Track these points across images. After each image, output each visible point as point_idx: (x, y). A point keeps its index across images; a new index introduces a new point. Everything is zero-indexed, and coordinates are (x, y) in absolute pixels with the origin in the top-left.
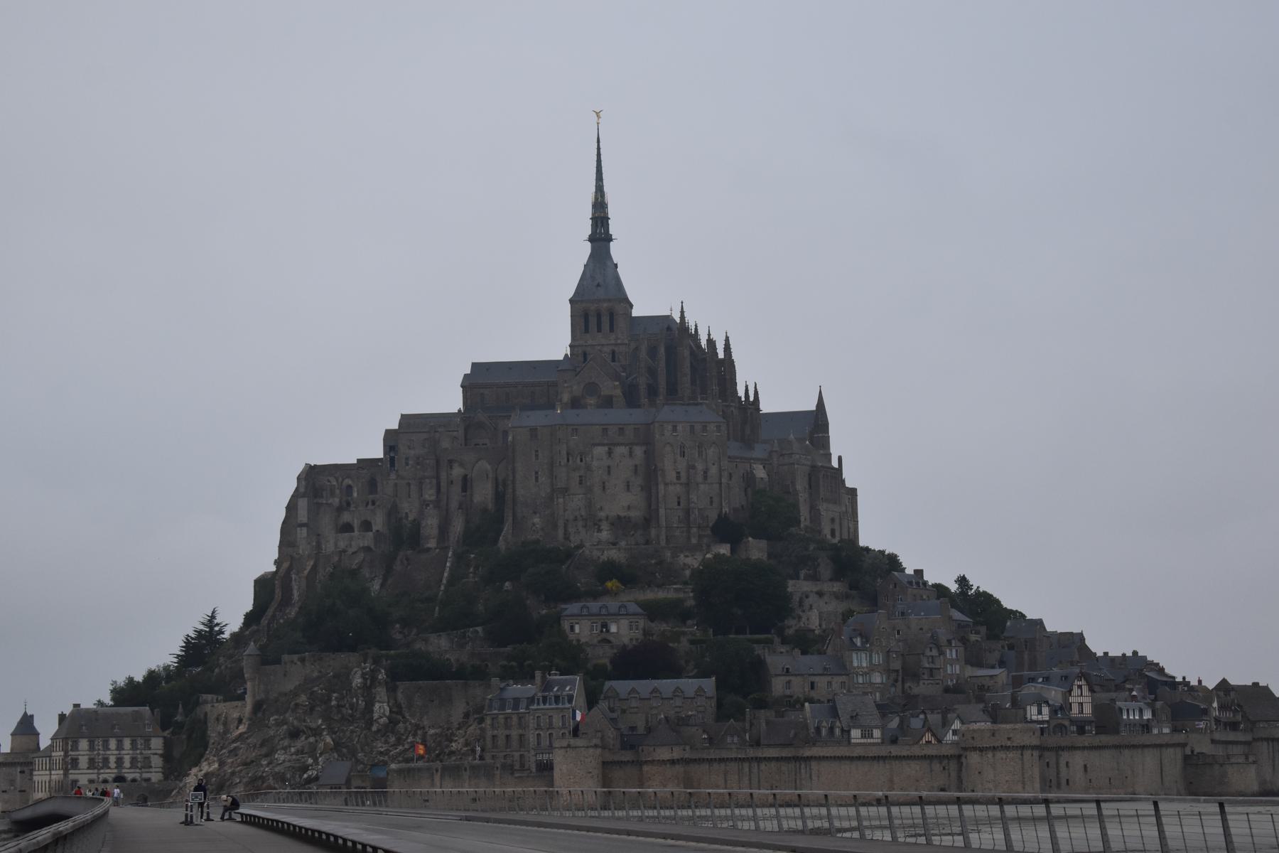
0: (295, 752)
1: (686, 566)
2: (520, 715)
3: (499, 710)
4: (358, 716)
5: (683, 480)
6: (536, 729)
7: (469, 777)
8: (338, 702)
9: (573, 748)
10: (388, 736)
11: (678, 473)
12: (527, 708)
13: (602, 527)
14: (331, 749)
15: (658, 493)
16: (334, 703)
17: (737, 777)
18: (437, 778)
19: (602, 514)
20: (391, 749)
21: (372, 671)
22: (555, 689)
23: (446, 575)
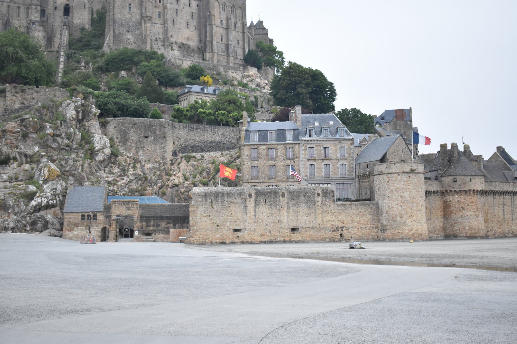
0: (8, 179)
1: (234, 79)
2: (288, 146)
3: (259, 141)
4: (74, 146)
5: (224, 25)
6: (308, 160)
7: (288, 203)
8: (54, 130)
9: (416, 173)
10: (111, 167)
11: (222, 21)
12: (296, 138)
13: (174, 48)
14: (58, 176)
15: (212, 30)
16: (49, 131)
17: (510, 209)
18: (251, 204)
19: (173, 40)
20: (118, 179)
21: (82, 105)
22: (317, 123)
23: (61, 66)
